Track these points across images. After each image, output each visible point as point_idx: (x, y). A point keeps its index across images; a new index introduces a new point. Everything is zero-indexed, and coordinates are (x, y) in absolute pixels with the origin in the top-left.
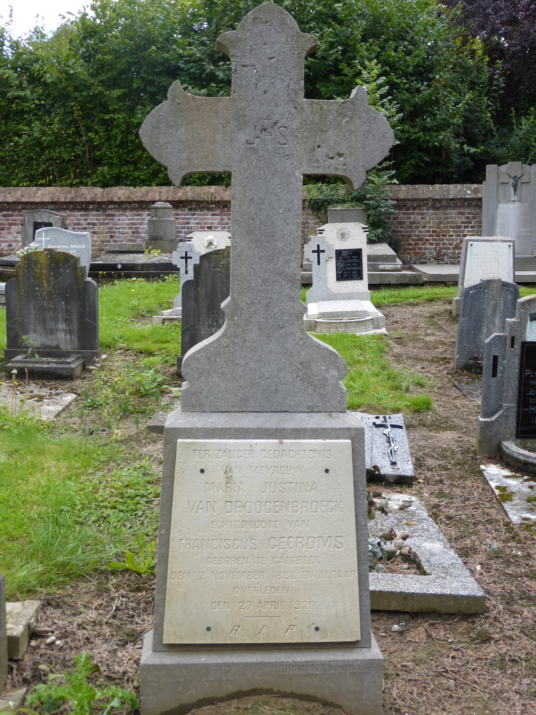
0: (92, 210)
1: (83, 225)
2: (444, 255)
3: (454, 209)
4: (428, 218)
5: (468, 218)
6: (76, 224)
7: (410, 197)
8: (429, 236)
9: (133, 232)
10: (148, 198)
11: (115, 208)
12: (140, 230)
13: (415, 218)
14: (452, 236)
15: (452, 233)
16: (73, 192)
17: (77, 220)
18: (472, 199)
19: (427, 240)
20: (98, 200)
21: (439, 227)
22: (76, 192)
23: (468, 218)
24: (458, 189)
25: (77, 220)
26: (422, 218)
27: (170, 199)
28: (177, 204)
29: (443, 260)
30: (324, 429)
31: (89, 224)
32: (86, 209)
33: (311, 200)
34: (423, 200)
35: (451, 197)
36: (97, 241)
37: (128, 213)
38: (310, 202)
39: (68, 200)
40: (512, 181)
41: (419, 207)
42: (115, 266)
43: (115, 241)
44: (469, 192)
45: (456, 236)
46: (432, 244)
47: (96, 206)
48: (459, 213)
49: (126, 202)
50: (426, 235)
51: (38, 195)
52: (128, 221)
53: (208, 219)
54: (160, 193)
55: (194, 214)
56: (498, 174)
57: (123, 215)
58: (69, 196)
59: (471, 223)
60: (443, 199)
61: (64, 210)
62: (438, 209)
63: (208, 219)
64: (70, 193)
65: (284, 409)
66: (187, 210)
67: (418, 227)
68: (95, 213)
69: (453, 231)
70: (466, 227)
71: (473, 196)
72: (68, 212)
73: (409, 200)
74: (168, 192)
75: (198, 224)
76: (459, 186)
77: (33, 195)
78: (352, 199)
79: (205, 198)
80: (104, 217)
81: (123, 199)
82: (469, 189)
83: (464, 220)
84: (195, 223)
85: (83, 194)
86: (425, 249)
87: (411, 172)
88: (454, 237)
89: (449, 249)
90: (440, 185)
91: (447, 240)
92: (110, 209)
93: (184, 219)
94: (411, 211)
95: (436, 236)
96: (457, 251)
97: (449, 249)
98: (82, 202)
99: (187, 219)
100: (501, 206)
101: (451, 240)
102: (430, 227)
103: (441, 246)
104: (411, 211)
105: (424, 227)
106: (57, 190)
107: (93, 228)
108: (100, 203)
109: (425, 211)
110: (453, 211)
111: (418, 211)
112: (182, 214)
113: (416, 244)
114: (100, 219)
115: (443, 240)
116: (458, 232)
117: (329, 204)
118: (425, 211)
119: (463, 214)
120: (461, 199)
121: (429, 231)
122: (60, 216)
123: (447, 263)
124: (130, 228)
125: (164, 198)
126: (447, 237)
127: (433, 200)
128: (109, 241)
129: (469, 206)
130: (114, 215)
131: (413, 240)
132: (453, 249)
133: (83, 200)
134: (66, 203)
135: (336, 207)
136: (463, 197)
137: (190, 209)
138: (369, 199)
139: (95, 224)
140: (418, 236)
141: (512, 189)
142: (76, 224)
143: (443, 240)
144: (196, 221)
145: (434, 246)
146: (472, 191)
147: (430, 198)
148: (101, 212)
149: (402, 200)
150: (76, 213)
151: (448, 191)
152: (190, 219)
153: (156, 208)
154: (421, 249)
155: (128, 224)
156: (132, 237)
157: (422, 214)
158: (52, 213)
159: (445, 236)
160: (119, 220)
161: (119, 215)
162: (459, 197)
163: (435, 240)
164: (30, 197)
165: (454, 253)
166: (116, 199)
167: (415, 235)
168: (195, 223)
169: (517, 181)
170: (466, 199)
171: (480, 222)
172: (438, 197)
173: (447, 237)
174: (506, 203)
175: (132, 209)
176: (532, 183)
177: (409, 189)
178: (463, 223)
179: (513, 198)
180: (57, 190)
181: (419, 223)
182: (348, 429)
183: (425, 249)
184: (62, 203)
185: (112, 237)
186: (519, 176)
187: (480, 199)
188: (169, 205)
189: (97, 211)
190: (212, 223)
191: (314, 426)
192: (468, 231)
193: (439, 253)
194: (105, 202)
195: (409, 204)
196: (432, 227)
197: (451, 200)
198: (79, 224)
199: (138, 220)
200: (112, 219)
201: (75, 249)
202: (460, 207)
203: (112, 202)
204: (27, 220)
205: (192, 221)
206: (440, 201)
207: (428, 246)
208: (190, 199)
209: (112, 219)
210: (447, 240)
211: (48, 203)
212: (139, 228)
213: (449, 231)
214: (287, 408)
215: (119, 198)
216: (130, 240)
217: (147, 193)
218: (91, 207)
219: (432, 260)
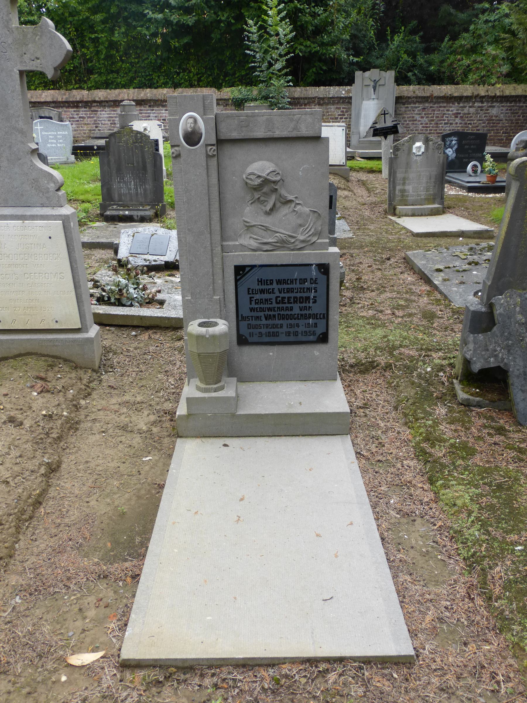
0: (82, 107)
1: (76, 118)
5: (343, 112)
6: (71, 118)
7: (302, 96)
9: (111, 124)
10: (119, 98)
11: (97, 106)
12: (116, 122)
16: (67, 94)
17: (72, 114)
18: (346, 98)
20: (85, 100)
22: (69, 94)
23: (343, 112)
24: (336, 90)
25: (72, 114)
27: (135, 98)
28: (140, 103)
30: (47, 215)
31: (80, 117)
32: (77, 107)
33: (233, 98)
34: (311, 98)
35: (331, 96)
36: (86, 130)
37: (107, 109)
38: (232, 100)
39: (64, 100)
40: (372, 84)
41: (309, 104)
42: (93, 146)
43: (99, 130)
44: (343, 92)
47: (84, 104)
48: (337, 108)
49: (105, 101)
51: (43, 96)
52: (107, 116)
53: (163, 113)
54: (128, 94)
55: (153, 110)
57: (103, 111)
58: (64, 97)
59: (344, 115)
60: (326, 97)
61: (62, 107)
63: (163, 113)
64: (65, 94)
65: (28, 205)
66: (147, 106)
68: (83, 109)
70: (341, 118)
71: (346, 95)
72: (65, 109)
73: (301, 98)
74: (134, 93)
75: (156, 117)
76: (337, 88)
77: (39, 96)
78: (262, 98)
79: (160, 98)
80: (90, 112)
81: (102, 99)
82: (344, 90)
83: (340, 113)
84: (153, 117)
85: (74, 95)
87: (313, 77)
90: (324, 87)
92: (94, 106)
93: (146, 113)
94: (303, 107)
98: (73, 101)
99: (148, 113)
100: (364, 102)
104: (303, 107)
106: (56, 93)
107: (82, 121)
108: (87, 102)
109: (313, 107)
110: (332, 107)
112: (145, 110)
114: (87, 114)
117: (246, 102)
119: (339, 108)
120: (337, 97)
122: (57, 111)
124: (109, 121)
125: (131, 98)
127: (319, 98)
128: (94, 130)
129: (343, 102)
130: (97, 111)
133: (74, 100)
134: (63, 102)
135: (250, 103)
136: (339, 96)
137: (150, 106)
138: (272, 98)
139: (85, 118)
141: (372, 89)
142: (71, 118)
144: (155, 115)
146: (346, 91)
148: (88, 109)
149: (297, 98)
150: (70, 110)
151: (329, 91)
152: (150, 113)
153: (124, 105)
155: (107, 118)
156: (111, 127)
158: (51, 110)
160: (101, 114)
161: (100, 111)
162: (336, 96)
164: (37, 98)
166: (97, 99)
168: (153, 117)
170: (341, 98)
171: (350, 115)
172: (322, 96)
174: (368, 100)
175: (109, 106)
176: (387, 84)
177: (302, 90)
178: (339, 115)
179: (373, 96)
180: (56, 93)
182: (60, 215)
184: (60, 102)
185: (96, 127)
186: (377, 80)
187: (351, 98)
188: (134, 103)
189: (85, 108)
190: (165, 116)
191: (42, 214)
194: (90, 101)
195: (302, 101)
197: (331, 98)
198: (73, 118)
199: (114, 114)
200: (96, 114)
201: (60, 135)
202: (337, 103)
203: (95, 101)
204: (34, 115)
205: (152, 115)
206: (323, 99)
208: (149, 98)
209: (96, 114)
211: (50, 102)
212: (115, 120)
214: (29, 205)
215: (100, 98)
216: (110, 130)
217: (119, 94)
218: (80, 105)
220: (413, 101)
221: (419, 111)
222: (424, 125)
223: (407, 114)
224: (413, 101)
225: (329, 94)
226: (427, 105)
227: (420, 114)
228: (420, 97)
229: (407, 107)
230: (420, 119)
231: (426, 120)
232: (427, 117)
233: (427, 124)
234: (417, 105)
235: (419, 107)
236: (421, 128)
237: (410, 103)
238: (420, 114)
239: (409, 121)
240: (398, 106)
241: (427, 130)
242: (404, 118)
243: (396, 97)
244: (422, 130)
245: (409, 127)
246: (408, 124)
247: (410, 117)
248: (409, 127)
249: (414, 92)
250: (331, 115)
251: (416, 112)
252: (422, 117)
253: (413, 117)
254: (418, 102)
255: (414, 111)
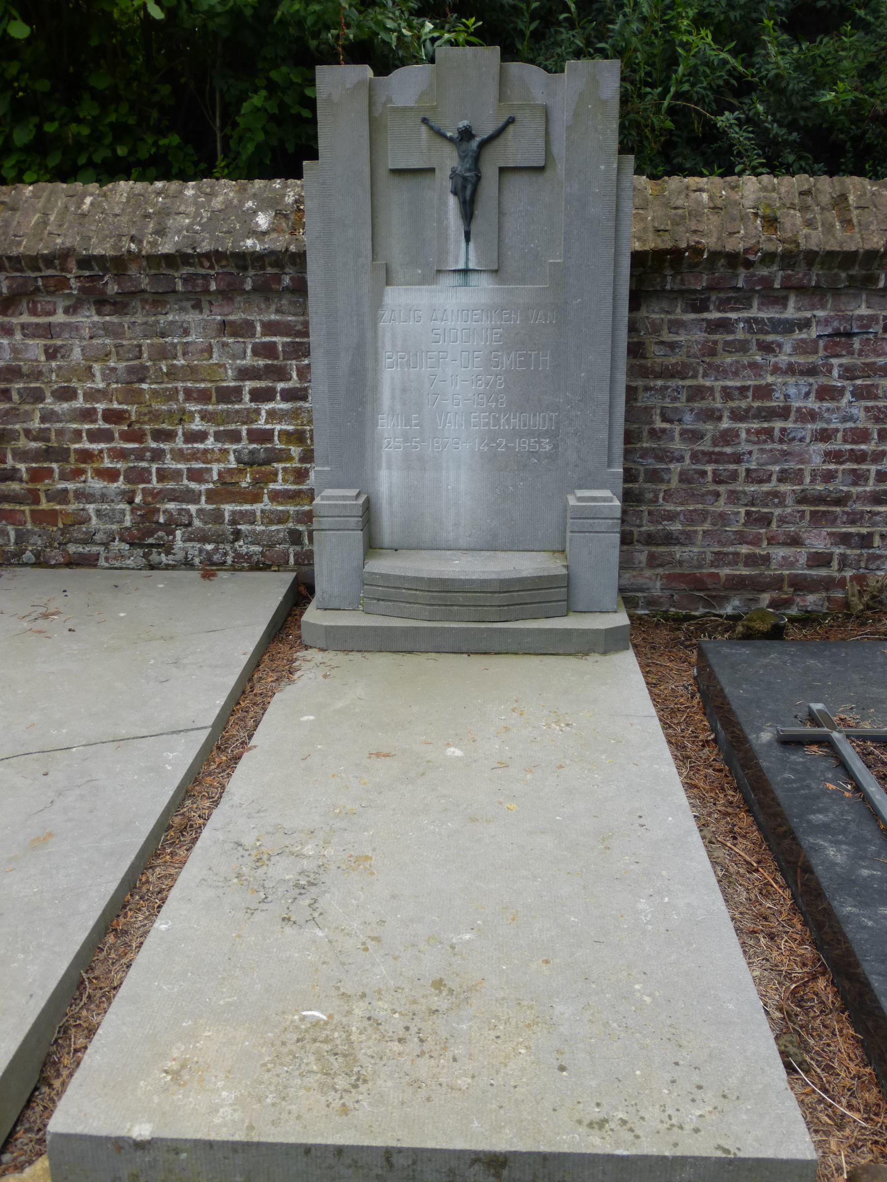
2: (170, 526)
3: (198, 307)
4: (77, 354)
5: (268, 350)
8: (94, 436)
13: (15, 350)
14: (201, 436)
15: (197, 425)
19: (86, 456)
21: (133, 396)
23: (268, 350)
24: (217, 203)
26: (51, 354)
29: (168, 550)
34: (35, 262)
35: (166, 248)
44: (263, 221)
45: (218, 436)
46: (111, 475)
48: (224, 327)
50: (78, 434)
56: (375, 125)
59: (282, 374)
62: (119, 305)
67: (37, 396)
69: (205, 416)
70: (259, 396)
71: (279, 242)
82: (265, 204)
83: (249, 361)
86: (80, 495)
88: (210, 443)
89: (192, 497)
90: (139, 186)
91: (179, 455)
95: (127, 437)
96: (228, 508)
97: (192, 497)
101: (194, 456)
102: (91, 395)
103: (155, 483)
105: (67, 394)
109: (60, 317)
110: (192, 317)
111: (26, 318)
113: (36, 475)
115: (158, 455)
116: (228, 417)
118: (60, 317)
119: (243, 329)
121: (88, 415)
123: (188, 564)
126: (180, 443)
127: (85, 262)
131: (22, 455)
132: (211, 496)
136: (228, 245)
140: (42, 435)
141: (452, 202)
143: (158, 455)
145: (120, 484)
147: (65, 255)
151: (165, 213)
154: (62, 496)
157: (48, 331)
159: (169, 436)
162: (205, 247)
163: (122, 455)
165: (217, 517)
167: (27, 432)
169: (477, 159)
173: (180, 443)
174: (424, 281)
176: (561, 168)
178: (245, 374)
181: (37, 375)
183: (80, 495)
187: (299, 259)
192: (272, 415)
193: (147, 514)
196: (101, 395)
197: (171, 260)
207: (97, 485)
210: (179, 455)
213: (183, 417)
219: (117, 545)
220: (767, 282)
221: (801, 348)
222: (837, 445)
223: (721, 372)
224: (767, 282)
225: (161, 232)
226: (863, 311)
227: (812, 371)
228: (811, 257)
229: (724, 326)
230: (812, 404)
231: (858, 410)
232: (860, 394)
233: (863, 436)
234: (791, 312)
235: (805, 324)
236: (817, 460)
237: (742, 299)
238: (812, 371)
239: (736, 416)
240: (654, 313)
241: (858, 478)
242: (697, 393)
243: (638, 258)
244: (829, 476)
245: (737, 459)
246: (728, 437)
247: (743, 390)
248: (737, 459)
249: (771, 222)
250: (192, 372)
251: (783, 359)
252: (826, 393)
253: (764, 392)
254: (801, 290)
255: (767, 348)
